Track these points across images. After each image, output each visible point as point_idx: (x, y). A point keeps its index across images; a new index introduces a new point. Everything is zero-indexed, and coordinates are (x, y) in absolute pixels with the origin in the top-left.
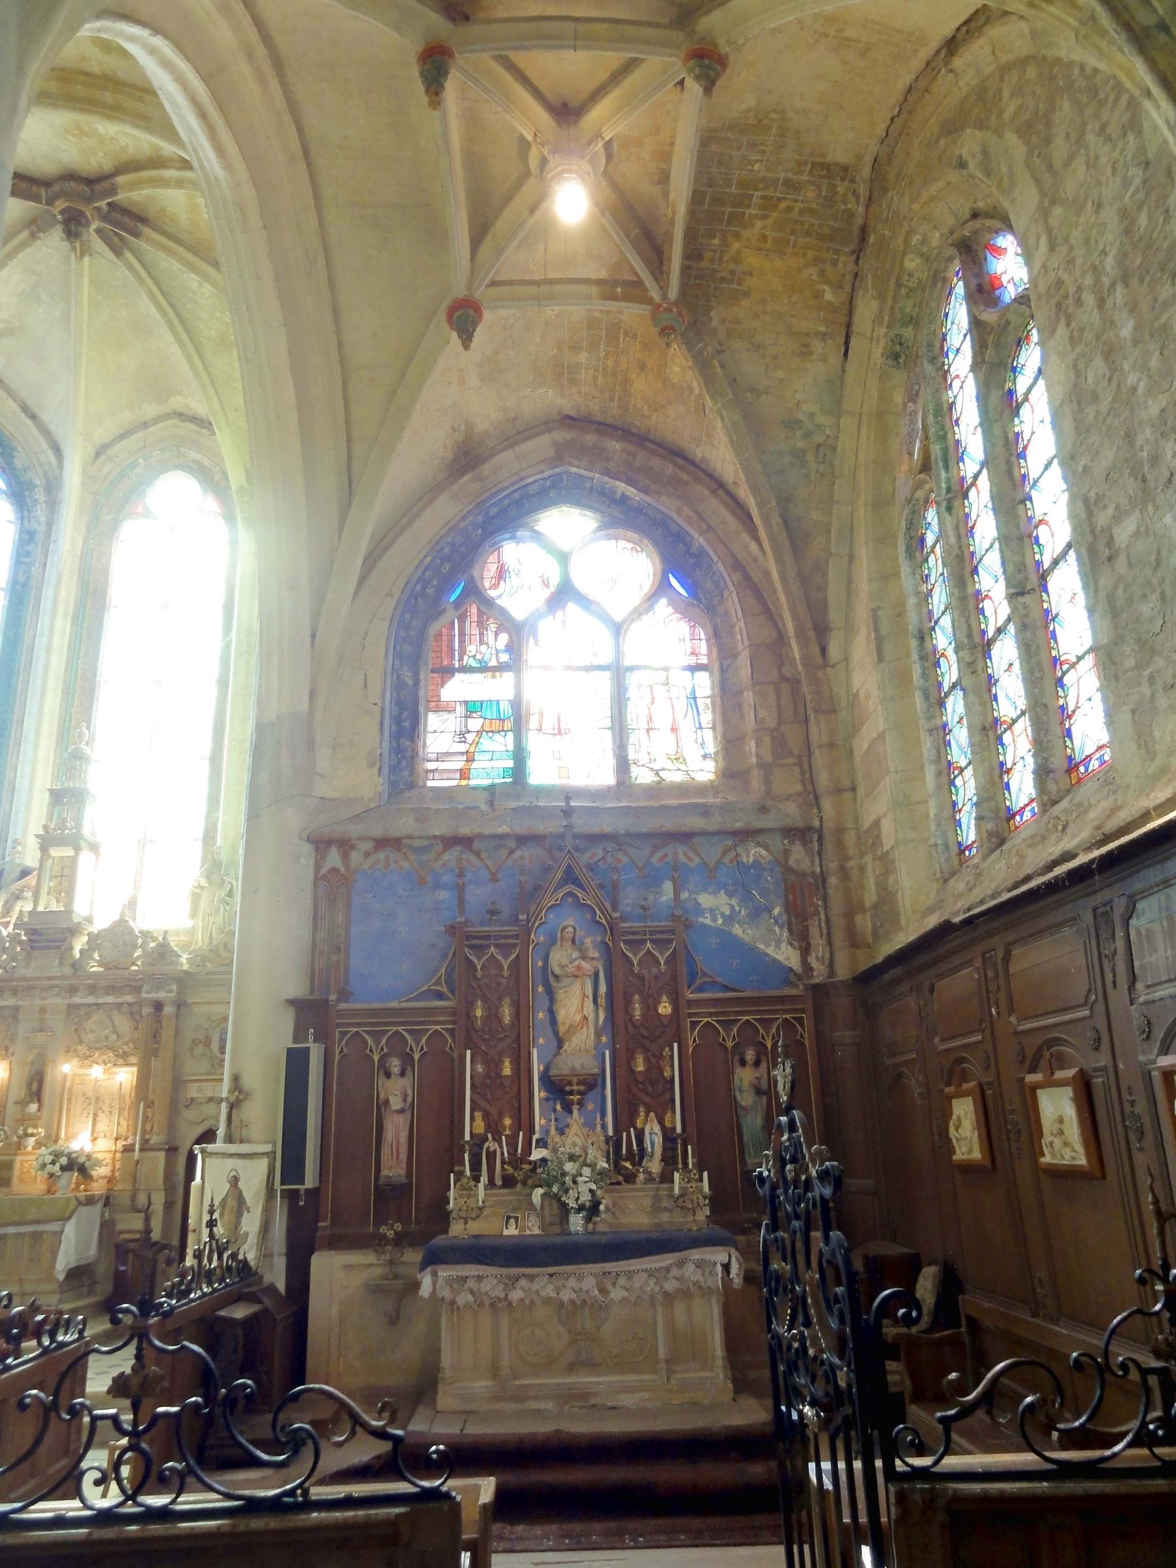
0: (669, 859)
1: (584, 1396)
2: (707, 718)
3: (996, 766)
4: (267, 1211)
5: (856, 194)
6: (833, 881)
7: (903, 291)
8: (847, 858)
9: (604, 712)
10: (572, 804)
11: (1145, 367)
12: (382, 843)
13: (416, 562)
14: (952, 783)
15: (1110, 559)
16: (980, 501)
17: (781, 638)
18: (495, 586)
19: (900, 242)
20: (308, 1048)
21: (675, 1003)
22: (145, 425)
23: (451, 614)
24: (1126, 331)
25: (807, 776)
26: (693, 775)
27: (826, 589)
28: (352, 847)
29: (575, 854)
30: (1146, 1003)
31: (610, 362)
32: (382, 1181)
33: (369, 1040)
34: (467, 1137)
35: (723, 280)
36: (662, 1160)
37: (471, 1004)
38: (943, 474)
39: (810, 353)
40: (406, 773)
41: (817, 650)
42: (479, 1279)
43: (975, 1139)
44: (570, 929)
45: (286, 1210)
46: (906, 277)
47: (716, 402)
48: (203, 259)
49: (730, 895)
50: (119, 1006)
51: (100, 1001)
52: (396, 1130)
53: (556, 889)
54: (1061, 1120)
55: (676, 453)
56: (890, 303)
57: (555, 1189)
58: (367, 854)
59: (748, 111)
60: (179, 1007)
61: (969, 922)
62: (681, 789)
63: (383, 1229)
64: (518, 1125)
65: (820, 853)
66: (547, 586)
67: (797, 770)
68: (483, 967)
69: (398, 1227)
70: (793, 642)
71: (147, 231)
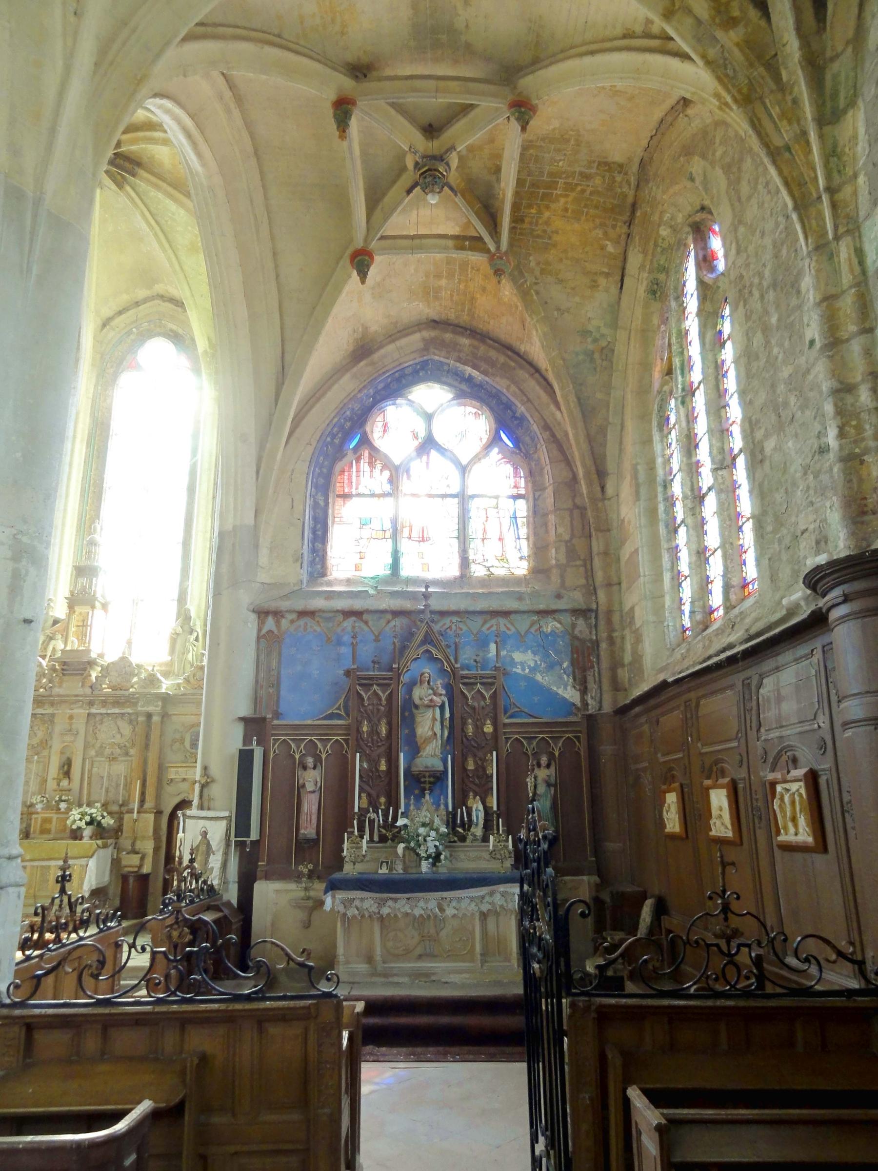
0: (494, 628)
1: (427, 975)
2: (523, 531)
3: (705, 578)
4: (226, 854)
5: (628, 183)
6: (604, 645)
7: (659, 249)
8: (613, 630)
9: (453, 526)
10: (430, 590)
11: (781, 345)
12: (302, 614)
13: (327, 422)
14: (680, 585)
15: (761, 461)
16: (700, 401)
17: (575, 478)
18: (382, 437)
19: (656, 217)
20: (252, 750)
21: (495, 724)
22: (137, 304)
23: (350, 456)
24: (774, 320)
25: (589, 573)
26: (513, 571)
27: (605, 446)
28: (282, 616)
29: (432, 625)
30: (766, 740)
31: (462, 286)
32: (300, 836)
33: (293, 745)
34: (356, 810)
35: (538, 236)
36: (484, 828)
37: (359, 724)
38: (680, 379)
39: (598, 286)
40: (319, 566)
41: (599, 489)
42: (362, 900)
43: (677, 820)
44: (427, 675)
45: (238, 853)
46: (661, 241)
47: (533, 319)
48: (180, 192)
49: (535, 653)
50: (123, 714)
51: (109, 712)
52: (310, 805)
53: (419, 646)
54: (721, 809)
55: (507, 348)
56: (649, 257)
57: (412, 844)
58: (292, 622)
59: (554, 130)
60: (163, 717)
61: (678, 681)
62: (504, 581)
63: (301, 868)
64: (389, 804)
65: (596, 626)
66: (417, 438)
67: (582, 569)
68: (369, 698)
69: (310, 866)
70: (582, 482)
71: (142, 172)
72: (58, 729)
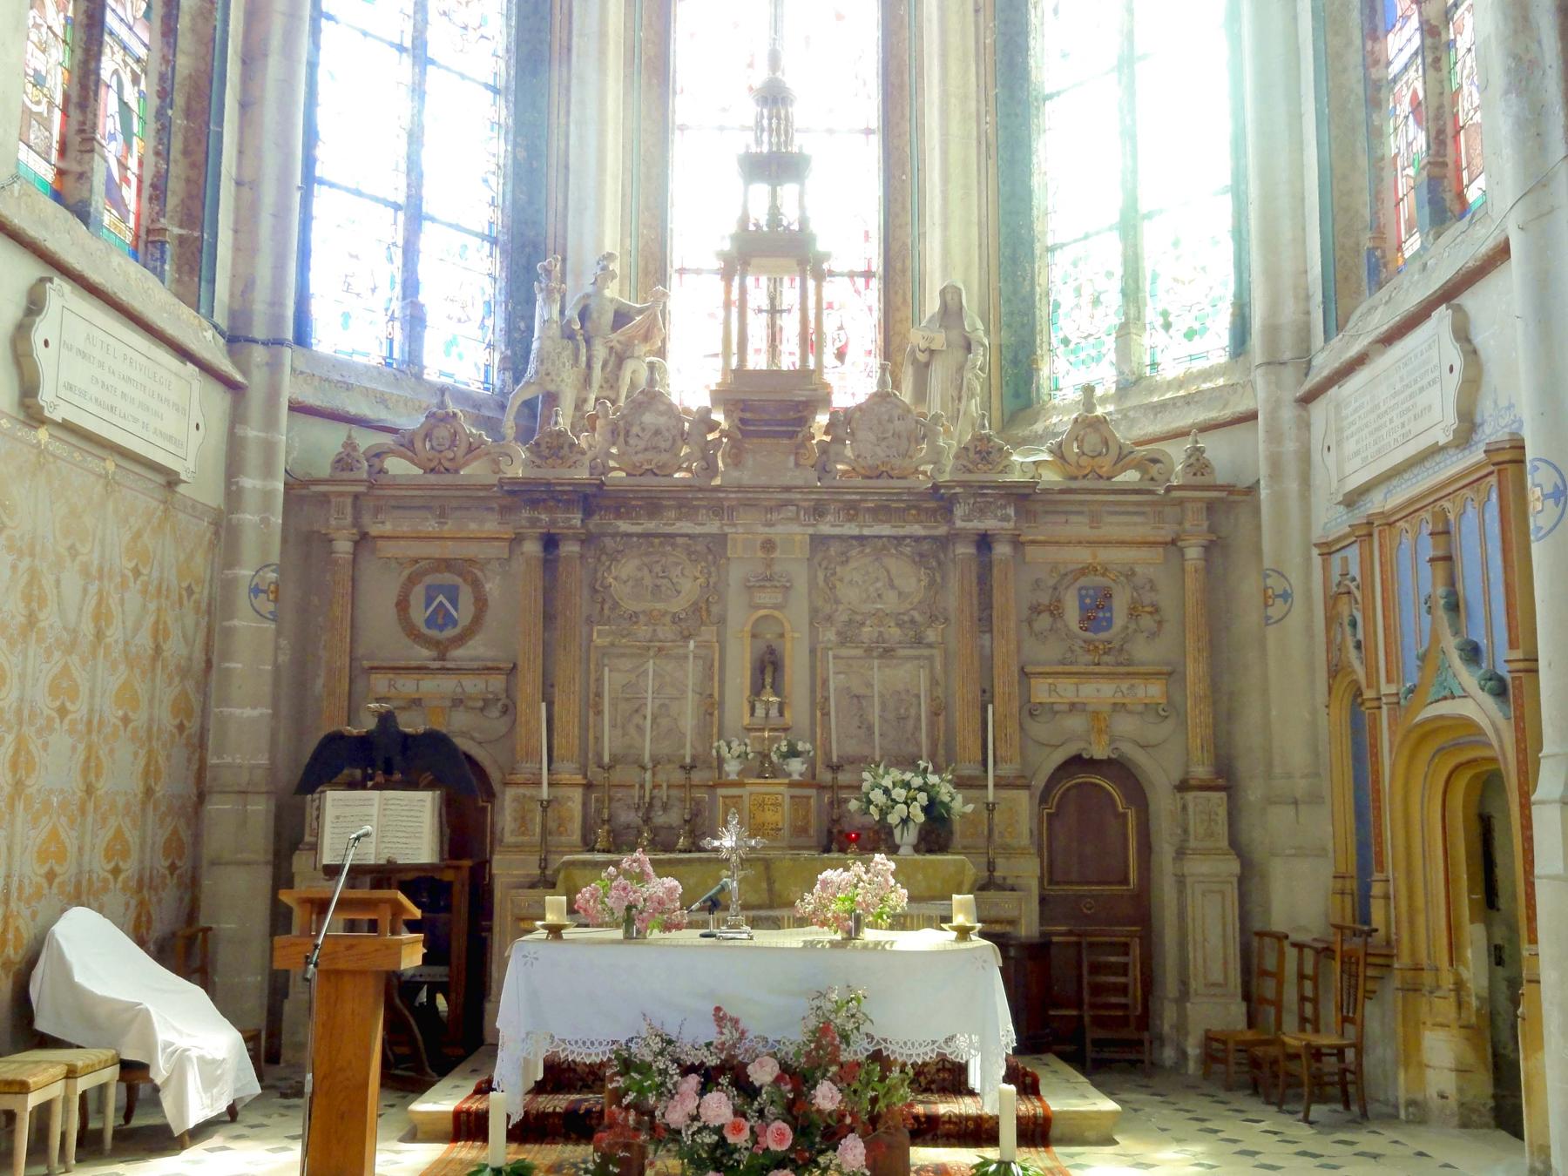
50: (899, 539)
51: (866, 532)
72: (736, 574)
